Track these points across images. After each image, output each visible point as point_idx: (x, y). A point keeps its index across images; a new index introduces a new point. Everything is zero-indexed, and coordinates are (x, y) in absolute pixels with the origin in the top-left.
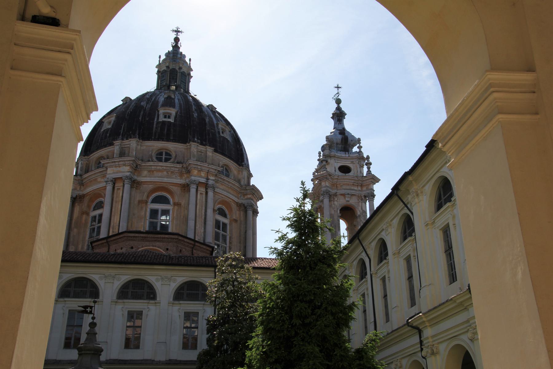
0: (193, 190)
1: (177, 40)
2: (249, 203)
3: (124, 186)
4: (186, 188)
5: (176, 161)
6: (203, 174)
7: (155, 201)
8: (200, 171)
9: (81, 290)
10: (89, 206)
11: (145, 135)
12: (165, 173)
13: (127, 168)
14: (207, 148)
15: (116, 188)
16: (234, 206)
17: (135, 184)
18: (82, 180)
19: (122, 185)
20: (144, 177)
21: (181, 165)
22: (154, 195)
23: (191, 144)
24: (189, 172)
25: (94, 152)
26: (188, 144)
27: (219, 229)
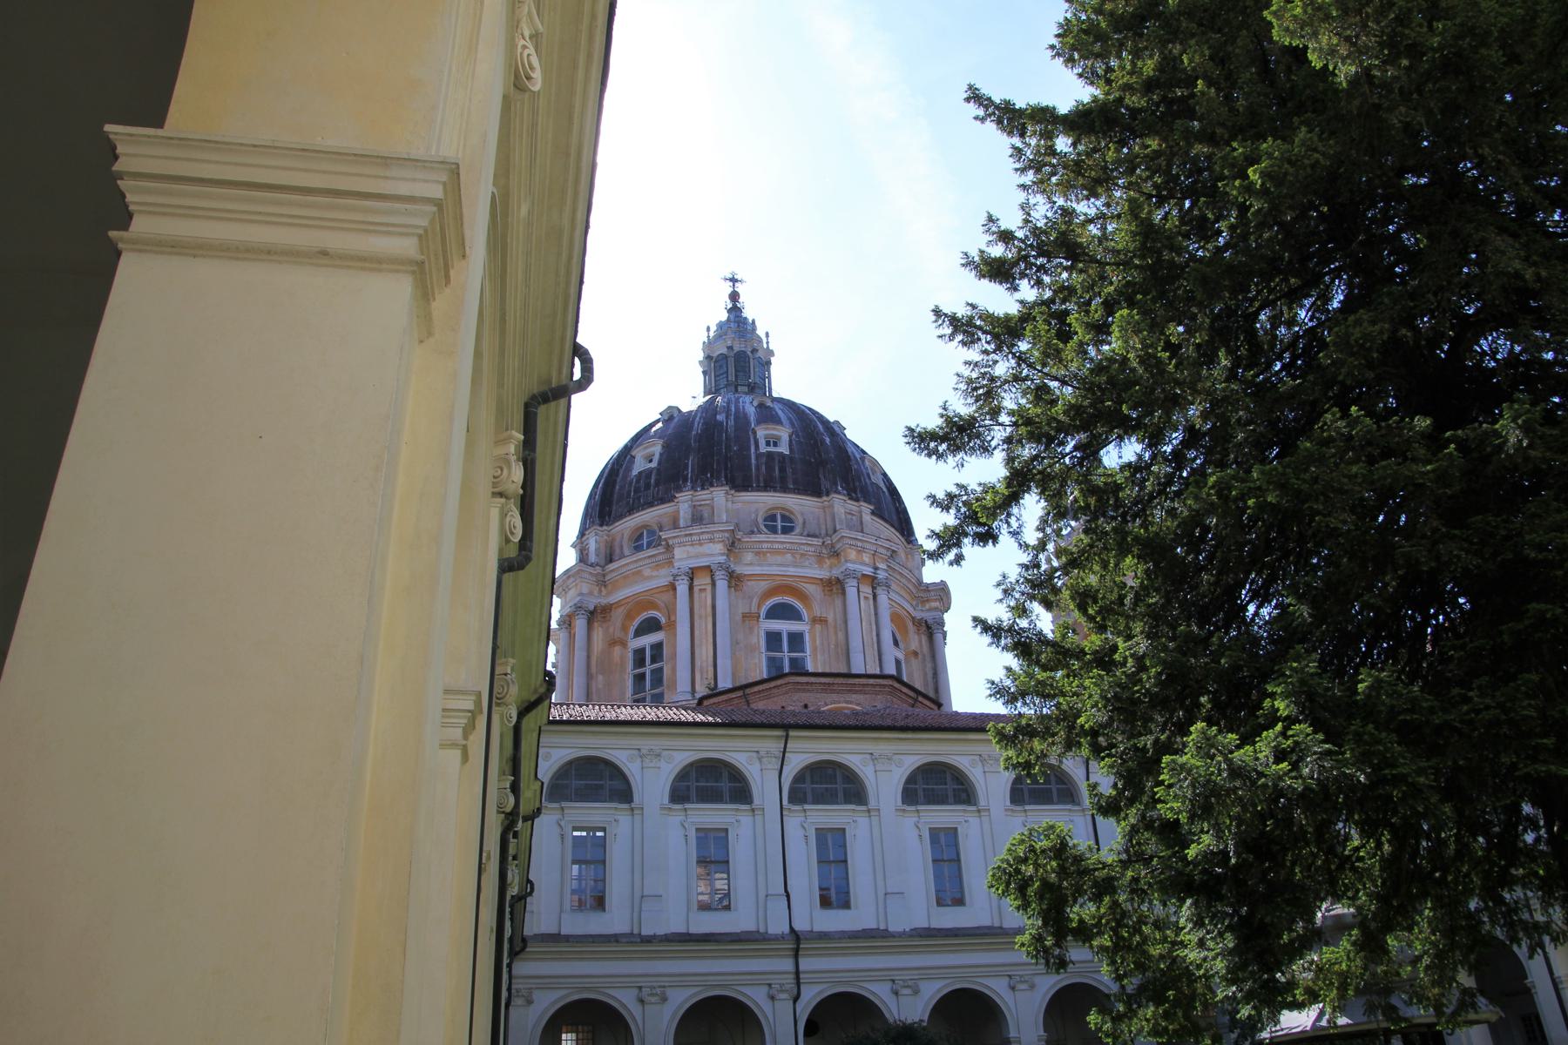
0: (851, 591)
1: (734, 296)
3: (714, 584)
4: (835, 586)
5: (805, 533)
6: (866, 558)
8: (861, 551)
10: (625, 628)
11: (740, 481)
12: (789, 556)
13: (719, 548)
15: (696, 589)
17: (735, 580)
18: (604, 576)
19: (708, 580)
20: (747, 565)
21: (821, 540)
24: (836, 554)
25: (621, 517)
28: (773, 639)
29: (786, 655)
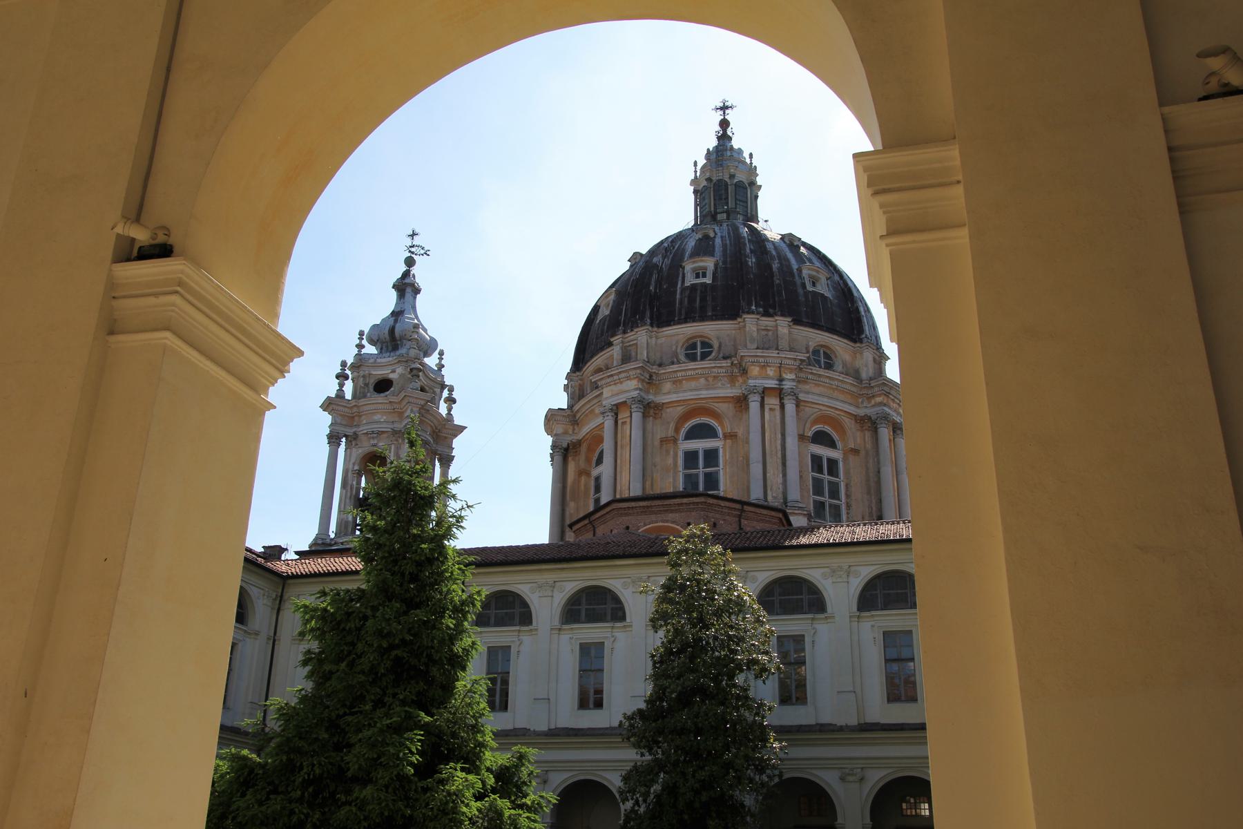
0: (754, 406)
1: (724, 124)
2: (879, 412)
4: (741, 402)
5: (721, 355)
6: (771, 372)
7: (691, 435)
8: (764, 367)
9: (506, 613)
11: (662, 320)
12: (702, 381)
13: (633, 384)
14: (777, 320)
15: (620, 422)
16: (848, 423)
17: (650, 410)
18: (575, 416)
20: (667, 395)
21: (729, 361)
22: (688, 425)
23: (745, 318)
24: (744, 372)
25: (589, 361)
26: (739, 320)
27: (820, 471)
28: (691, 457)
29: (701, 470)
